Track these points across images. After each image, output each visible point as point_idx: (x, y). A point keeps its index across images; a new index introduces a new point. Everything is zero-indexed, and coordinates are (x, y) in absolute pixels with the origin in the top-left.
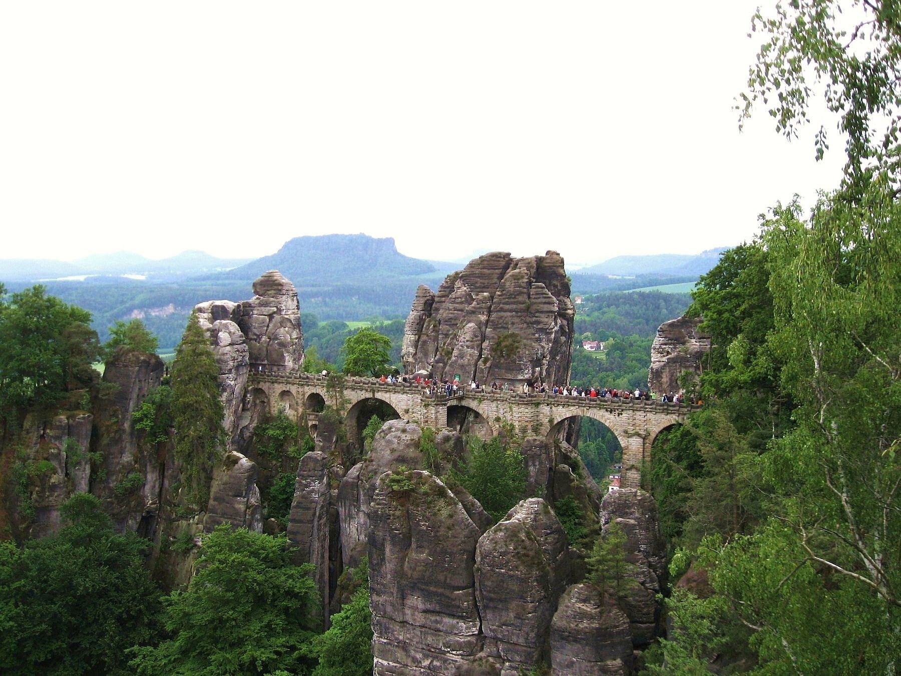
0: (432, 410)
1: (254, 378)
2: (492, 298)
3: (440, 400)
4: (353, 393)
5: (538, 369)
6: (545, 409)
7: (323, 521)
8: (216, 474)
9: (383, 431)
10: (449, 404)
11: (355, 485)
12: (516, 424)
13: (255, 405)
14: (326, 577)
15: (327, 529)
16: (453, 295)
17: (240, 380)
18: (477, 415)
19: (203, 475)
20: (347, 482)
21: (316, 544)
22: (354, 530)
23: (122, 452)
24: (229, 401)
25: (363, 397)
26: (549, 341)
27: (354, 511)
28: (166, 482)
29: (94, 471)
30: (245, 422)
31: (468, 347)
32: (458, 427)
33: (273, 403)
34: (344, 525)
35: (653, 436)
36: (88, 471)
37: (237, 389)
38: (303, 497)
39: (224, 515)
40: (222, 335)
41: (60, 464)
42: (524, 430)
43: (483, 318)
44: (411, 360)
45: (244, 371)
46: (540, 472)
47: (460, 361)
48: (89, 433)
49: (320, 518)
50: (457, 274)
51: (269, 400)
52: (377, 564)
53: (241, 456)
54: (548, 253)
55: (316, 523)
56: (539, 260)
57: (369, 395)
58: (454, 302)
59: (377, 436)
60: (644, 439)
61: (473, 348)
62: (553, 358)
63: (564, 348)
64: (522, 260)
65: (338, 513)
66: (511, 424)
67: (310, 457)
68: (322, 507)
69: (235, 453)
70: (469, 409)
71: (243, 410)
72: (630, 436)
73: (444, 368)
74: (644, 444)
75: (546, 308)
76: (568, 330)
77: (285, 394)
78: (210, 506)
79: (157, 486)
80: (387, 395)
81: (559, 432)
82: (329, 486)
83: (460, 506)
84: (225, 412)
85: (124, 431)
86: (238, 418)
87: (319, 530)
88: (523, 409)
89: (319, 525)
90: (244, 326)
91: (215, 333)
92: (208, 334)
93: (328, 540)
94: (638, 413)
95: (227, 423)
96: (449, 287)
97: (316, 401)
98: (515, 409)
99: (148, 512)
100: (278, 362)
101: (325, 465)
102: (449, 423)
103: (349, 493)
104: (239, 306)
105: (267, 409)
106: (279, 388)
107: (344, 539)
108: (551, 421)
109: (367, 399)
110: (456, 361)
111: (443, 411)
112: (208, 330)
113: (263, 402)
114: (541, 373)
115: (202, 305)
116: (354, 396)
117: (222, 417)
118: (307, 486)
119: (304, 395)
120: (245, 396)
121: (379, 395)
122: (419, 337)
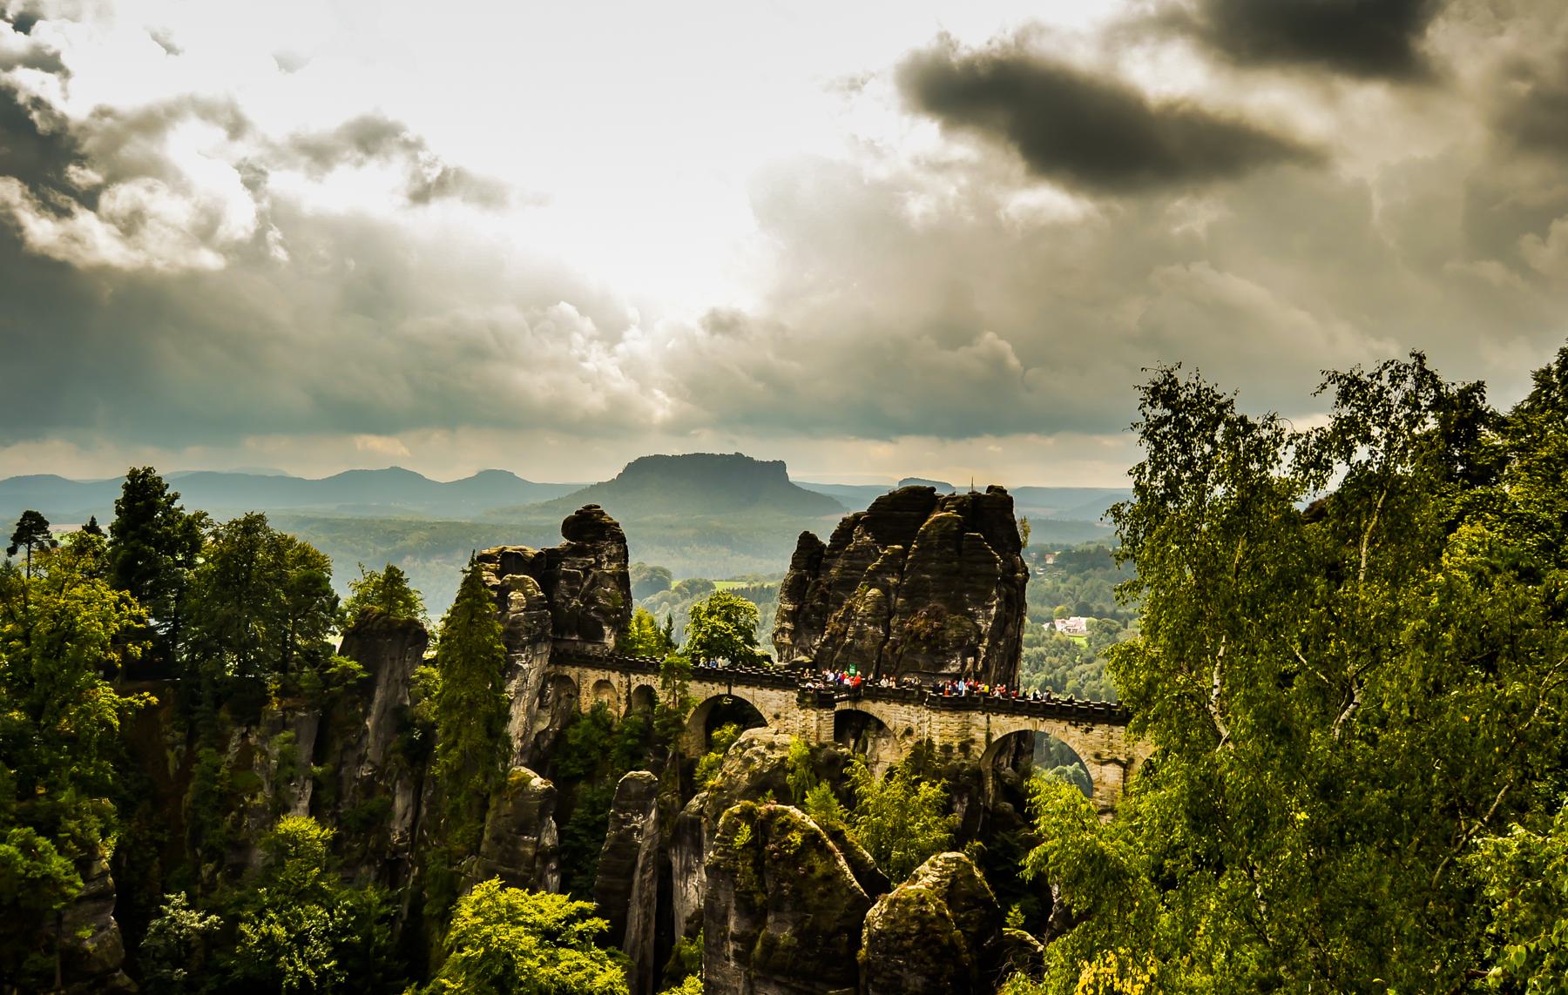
0: (812, 716)
1: (558, 658)
2: (905, 552)
3: (822, 701)
4: (700, 686)
5: (970, 660)
6: (979, 719)
7: (647, 876)
8: (493, 802)
9: (741, 745)
10: (839, 707)
11: (695, 824)
12: (937, 741)
13: (559, 699)
14: (650, 962)
15: (654, 888)
16: (851, 547)
17: (537, 663)
18: (880, 725)
19: (477, 801)
20: (685, 817)
21: (636, 912)
22: (692, 892)
23: (361, 760)
24: (519, 693)
25: (714, 693)
26: (988, 617)
27: (694, 862)
28: (424, 811)
29: (318, 785)
30: (542, 726)
31: (870, 624)
32: (852, 742)
33: (583, 697)
34: (678, 883)
35: (1138, 766)
36: (309, 791)
37: (532, 677)
38: (619, 838)
39: (502, 861)
40: (515, 595)
41: (268, 776)
42: (947, 749)
43: (893, 580)
44: (787, 640)
45: (545, 648)
46: (970, 815)
47: (858, 643)
48: (314, 734)
49: (644, 871)
50: (857, 516)
51: (578, 692)
52: (716, 945)
53: (531, 773)
54: (990, 488)
55: (637, 878)
56: (975, 497)
57: (723, 690)
58: (850, 558)
59: (731, 751)
60: (1126, 766)
61: (875, 624)
62: (994, 643)
63: (1010, 629)
64: (952, 498)
65: (670, 864)
66: (929, 740)
67: (632, 779)
68: (648, 854)
69: (524, 770)
70: (867, 718)
71: (541, 706)
72: (1103, 764)
73: (833, 654)
74: (1125, 775)
75: (983, 568)
76: (1014, 606)
77: (601, 685)
78: (483, 848)
79: (409, 816)
80: (750, 691)
81: (1000, 753)
82: (660, 822)
83: (842, 862)
84: (513, 710)
85: (366, 732)
86: (532, 718)
87: (641, 889)
88: (946, 717)
89: (642, 881)
90: (547, 583)
91: (503, 591)
92: (495, 594)
93: (655, 903)
94: (1116, 729)
95: (515, 727)
96: (844, 532)
97: (647, 693)
98: (935, 717)
99: (394, 854)
100: (596, 636)
101: (651, 791)
102: (839, 735)
103: (683, 834)
104: (539, 554)
105: (574, 707)
106: (593, 676)
107: (677, 904)
108: (989, 736)
109: (720, 697)
110: (851, 644)
111: (828, 716)
112: (494, 588)
113: (570, 696)
114: (975, 663)
115: (486, 552)
116: (700, 692)
117: (507, 718)
118: (625, 822)
119: (629, 686)
120: (544, 686)
121: (739, 691)
122: (800, 608)
